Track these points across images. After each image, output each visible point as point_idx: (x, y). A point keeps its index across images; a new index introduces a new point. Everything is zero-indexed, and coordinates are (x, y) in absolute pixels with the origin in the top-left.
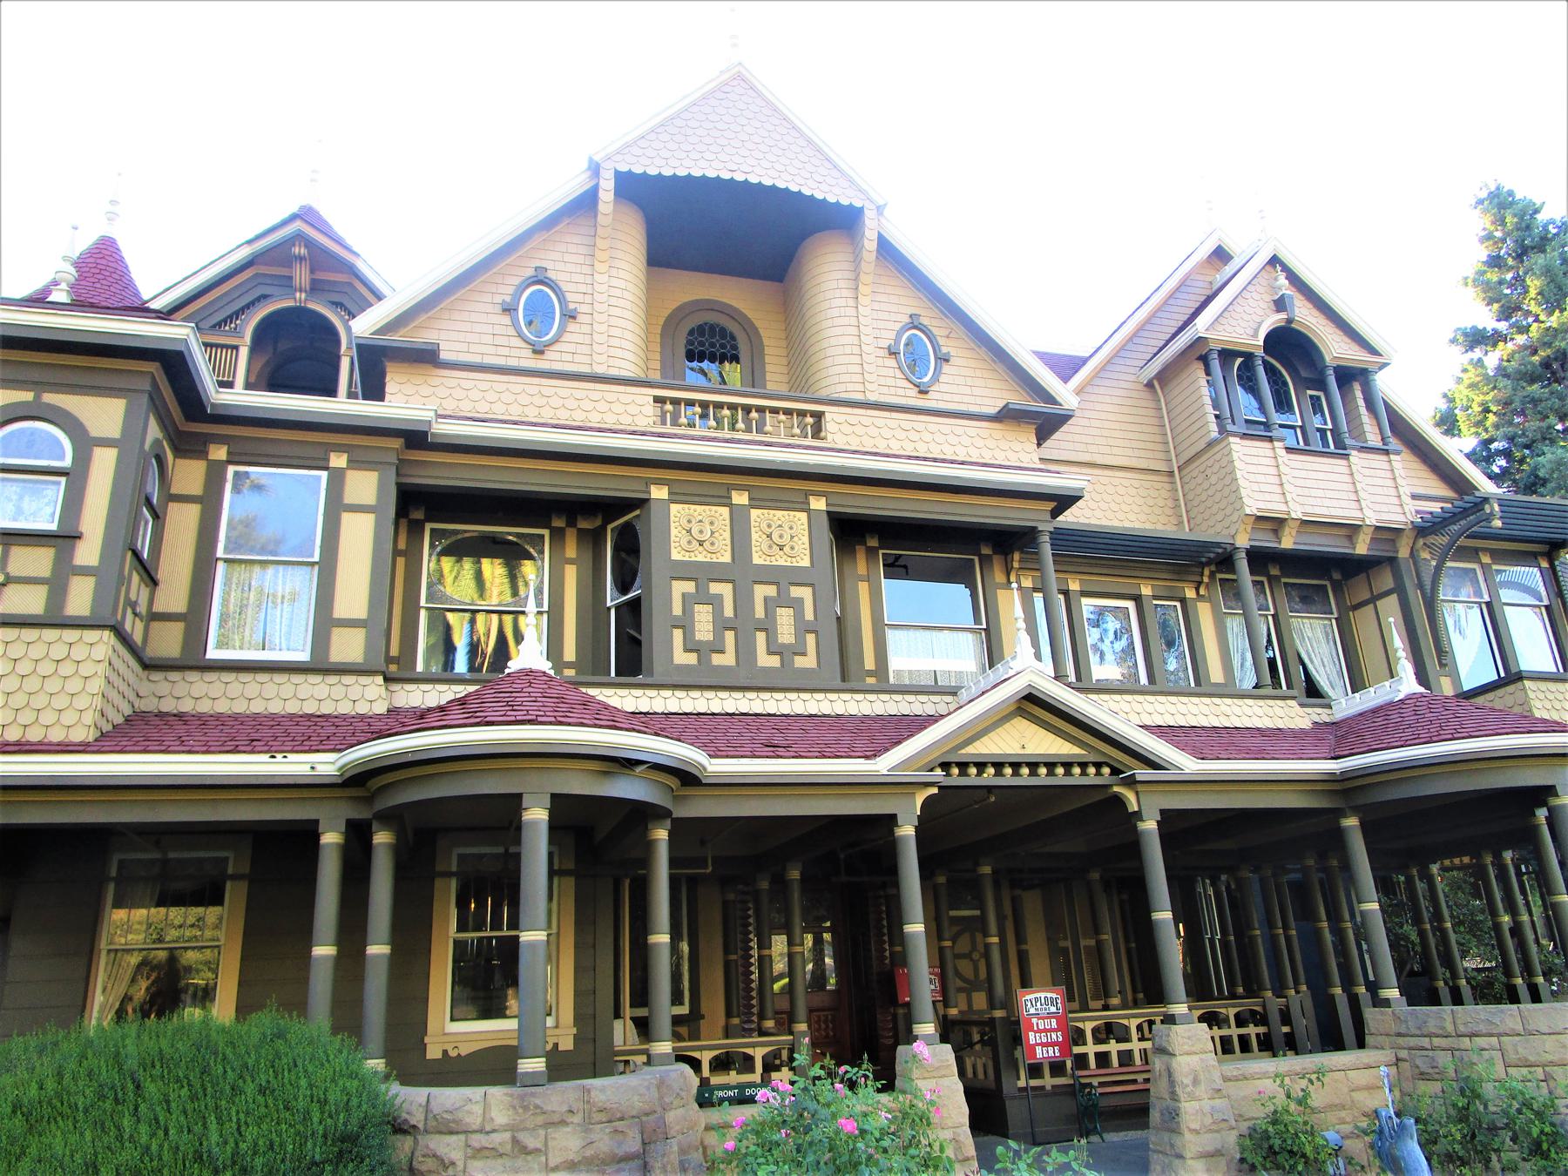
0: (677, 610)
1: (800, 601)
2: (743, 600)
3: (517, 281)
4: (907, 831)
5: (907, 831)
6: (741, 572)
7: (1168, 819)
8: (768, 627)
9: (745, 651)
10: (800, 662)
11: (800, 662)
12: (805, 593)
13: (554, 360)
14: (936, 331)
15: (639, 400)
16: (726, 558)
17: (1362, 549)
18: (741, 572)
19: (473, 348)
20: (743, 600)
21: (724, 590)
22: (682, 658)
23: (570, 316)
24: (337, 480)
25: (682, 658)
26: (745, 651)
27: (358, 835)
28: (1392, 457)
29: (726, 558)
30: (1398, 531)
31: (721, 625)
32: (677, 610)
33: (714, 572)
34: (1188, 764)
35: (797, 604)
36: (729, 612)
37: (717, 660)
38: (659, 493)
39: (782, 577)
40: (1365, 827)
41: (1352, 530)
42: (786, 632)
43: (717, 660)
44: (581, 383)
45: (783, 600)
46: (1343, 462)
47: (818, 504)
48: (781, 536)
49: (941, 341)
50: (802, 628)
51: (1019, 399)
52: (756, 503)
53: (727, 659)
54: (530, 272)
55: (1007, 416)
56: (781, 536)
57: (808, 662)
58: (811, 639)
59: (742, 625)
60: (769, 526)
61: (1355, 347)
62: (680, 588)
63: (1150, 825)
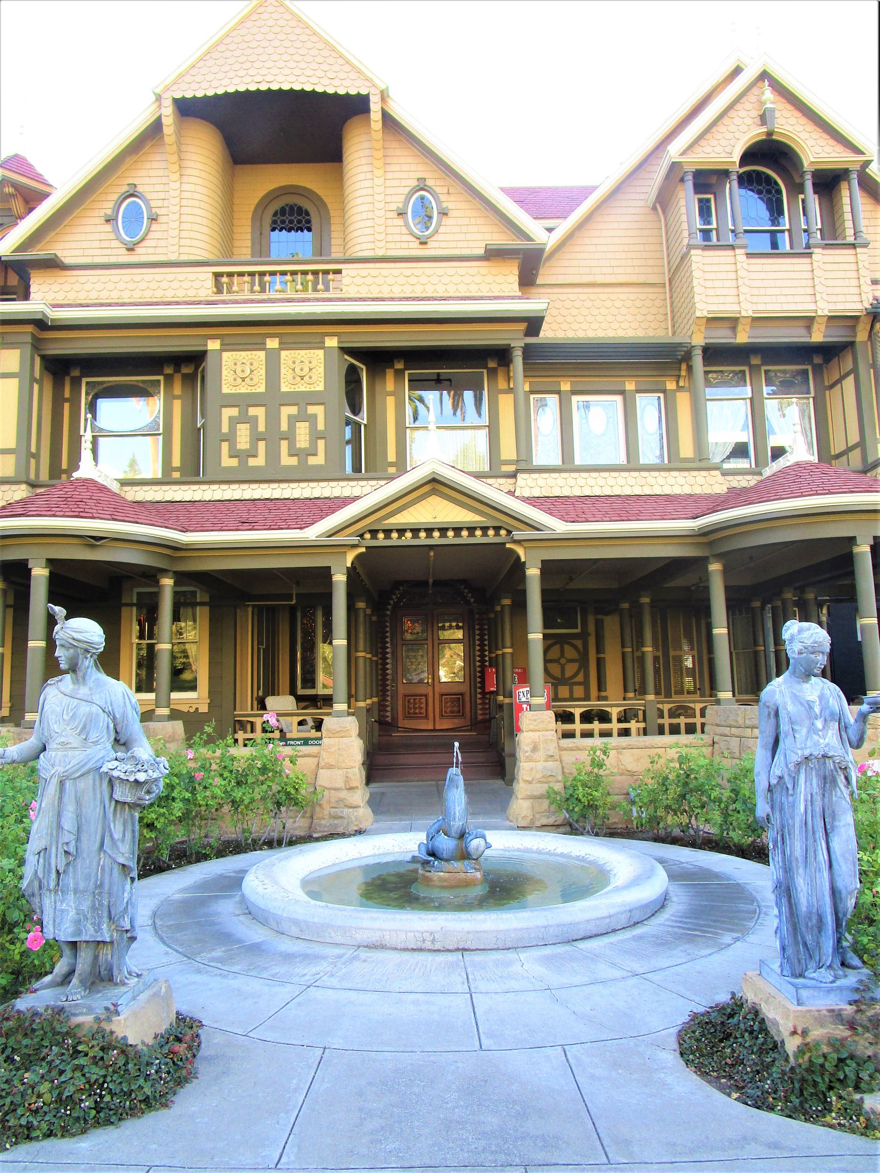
0: (225, 429)
1: (315, 416)
2: (273, 418)
3: (115, 197)
4: (340, 578)
5: (340, 578)
6: (272, 398)
7: (548, 568)
8: (290, 436)
9: (273, 455)
10: (312, 461)
11: (312, 461)
12: (318, 411)
13: (143, 254)
14: (438, 190)
15: (202, 277)
16: (262, 389)
17: (818, 336)
18: (272, 398)
19: (87, 252)
20: (273, 418)
21: (259, 412)
22: (228, 462)
25: (228, 462)
26: (273, 455)
28: (859, 250)
29: (262, 389)
30: (856, 318)
31: (256, 437)
32: (225, 429)
33: (252, 400)
35: (312, 419)
36: (262, 427)
37: (252, 462)
38: (213, 345)
41: (809, 321)
42: (303, 439)
43: (252, 462)
45: (302, 416)
46: (807, 260)
47: (332, 342)
48: (302, 370)
49: (443, 198)
50: (315, 436)
51: (501, 239)
52: (284, 346)
53: (259, 461)
54: (125, 188)
55: (493, 255)
56: (302, 370)
57: (318, 460)
58: (321, 444)
59: (273, 437)
60: (294, 362)
61: (839, 148)
63: (533, 572)
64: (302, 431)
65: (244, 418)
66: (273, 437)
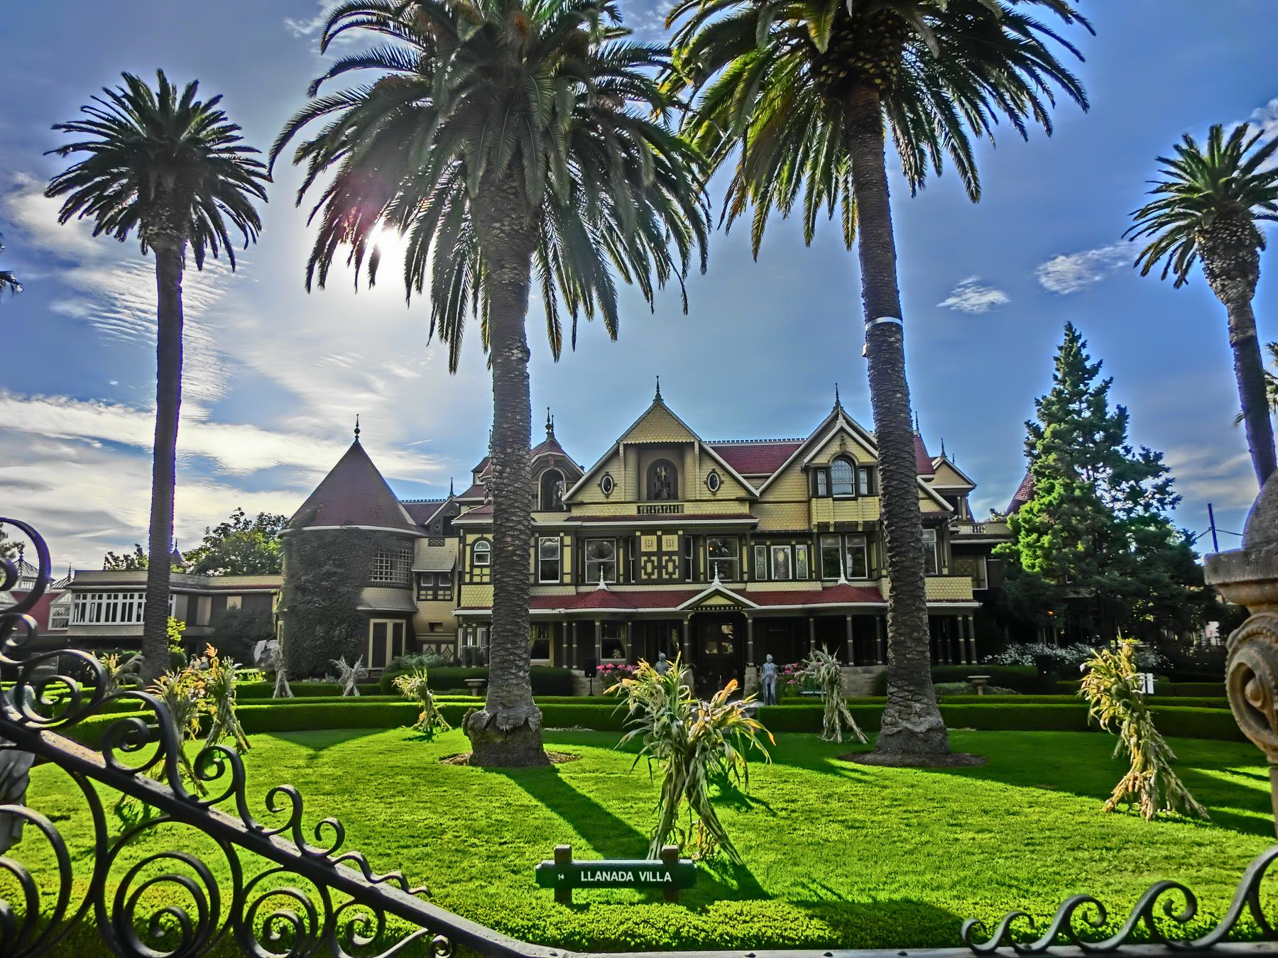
2: (660, 560)
6: (660, 553)
8: (666, 567)
9: (660, 574)
18: (660, 553)
20: (660, 560)
22: (644, 577)
23: (615, 485)
24: (562, 539)
25: (644, 577)
26: (660, 574)
27: (570, 624)
31: (654, 567)
33: (652, 554)
34: (758, 607)
38: (638, 534)
39: (670, 554)
40: (815, 621)
42: (670, 569)
44: (618, 503)
47: (681, 533)
51: (742, 494)
53: (655, 577)
57: (676, 576)
59: (660, 567)
62: (644, 559)
64: (670, 565)
65: (649, 561)
66: (660, 567)
